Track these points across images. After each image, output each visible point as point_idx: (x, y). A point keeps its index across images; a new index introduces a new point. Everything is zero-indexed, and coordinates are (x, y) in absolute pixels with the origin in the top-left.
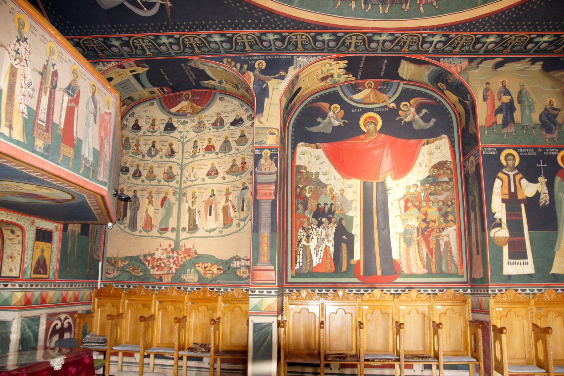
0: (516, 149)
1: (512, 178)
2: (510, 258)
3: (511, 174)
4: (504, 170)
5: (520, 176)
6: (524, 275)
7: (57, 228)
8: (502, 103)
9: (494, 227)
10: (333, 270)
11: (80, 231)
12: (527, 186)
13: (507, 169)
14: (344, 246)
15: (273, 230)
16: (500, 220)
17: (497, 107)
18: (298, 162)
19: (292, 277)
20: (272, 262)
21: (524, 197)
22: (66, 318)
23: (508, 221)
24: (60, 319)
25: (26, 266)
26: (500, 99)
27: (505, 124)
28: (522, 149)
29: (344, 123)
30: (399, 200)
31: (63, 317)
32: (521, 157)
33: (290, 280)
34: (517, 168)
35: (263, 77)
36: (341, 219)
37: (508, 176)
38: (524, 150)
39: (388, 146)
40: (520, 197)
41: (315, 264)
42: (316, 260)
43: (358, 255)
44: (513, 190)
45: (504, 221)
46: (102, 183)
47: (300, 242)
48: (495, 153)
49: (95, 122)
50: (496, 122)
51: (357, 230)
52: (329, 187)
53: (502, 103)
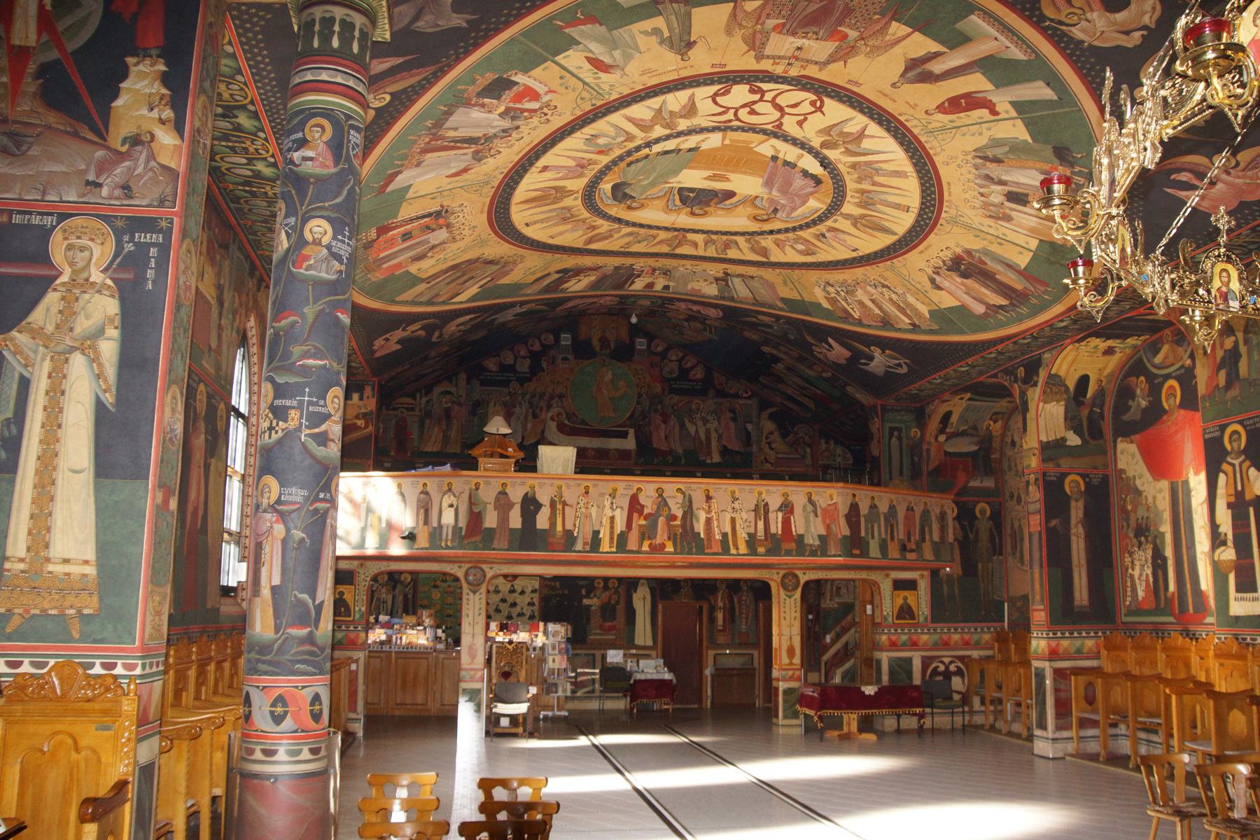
0: (1241, 423)
1: (1237, 468)
2: (1238, 590)
3: (1236, 462)
4: (1229, 459)
5: (1247, 463)
6: (1254, 616)
7: (922, 576)
8: (1225, 351)
9: (1218, 547)
10: (1154, 606)
11: (960, 573)
12: (1256, 479)
13: (1233, 456)
14: (1160, 572)
15: (1041, 566)
16: (1226, 534)
17: (1218, 360)
18: (1121, 465)
19: (1125, 615)
20: (1042, 600)
21: (1252, 497)
22: (951, 662)
23: (1234, 536)
24: (943, 662)
25: (885, 613)
26: (1222, 346)
27: (1228, 386)
28: (1249, 419)
29: (1150, 401)
30: (1201, 504)
31: (947, 660)
32: (1248, 433)
33: (1125, 619)
34: (1245, 452)
35: (1024, 386)
36: (1156, 537)
37: (1233, 465)
38: (1251, 422)
39: (1187, 426)
40: (1248, 497)
41: (1140, 598)
42: (1141, 594)
43: (1172, 587)
44: (1239, 488)
45: (1230, 536)
46: (835, 556)
47: (1127, 570)
48: (1218, 434)
49: (816, 516)
50: (1218, 385)
51: (1169, 552)
52: (1144, 494)
53: (1225, 351)
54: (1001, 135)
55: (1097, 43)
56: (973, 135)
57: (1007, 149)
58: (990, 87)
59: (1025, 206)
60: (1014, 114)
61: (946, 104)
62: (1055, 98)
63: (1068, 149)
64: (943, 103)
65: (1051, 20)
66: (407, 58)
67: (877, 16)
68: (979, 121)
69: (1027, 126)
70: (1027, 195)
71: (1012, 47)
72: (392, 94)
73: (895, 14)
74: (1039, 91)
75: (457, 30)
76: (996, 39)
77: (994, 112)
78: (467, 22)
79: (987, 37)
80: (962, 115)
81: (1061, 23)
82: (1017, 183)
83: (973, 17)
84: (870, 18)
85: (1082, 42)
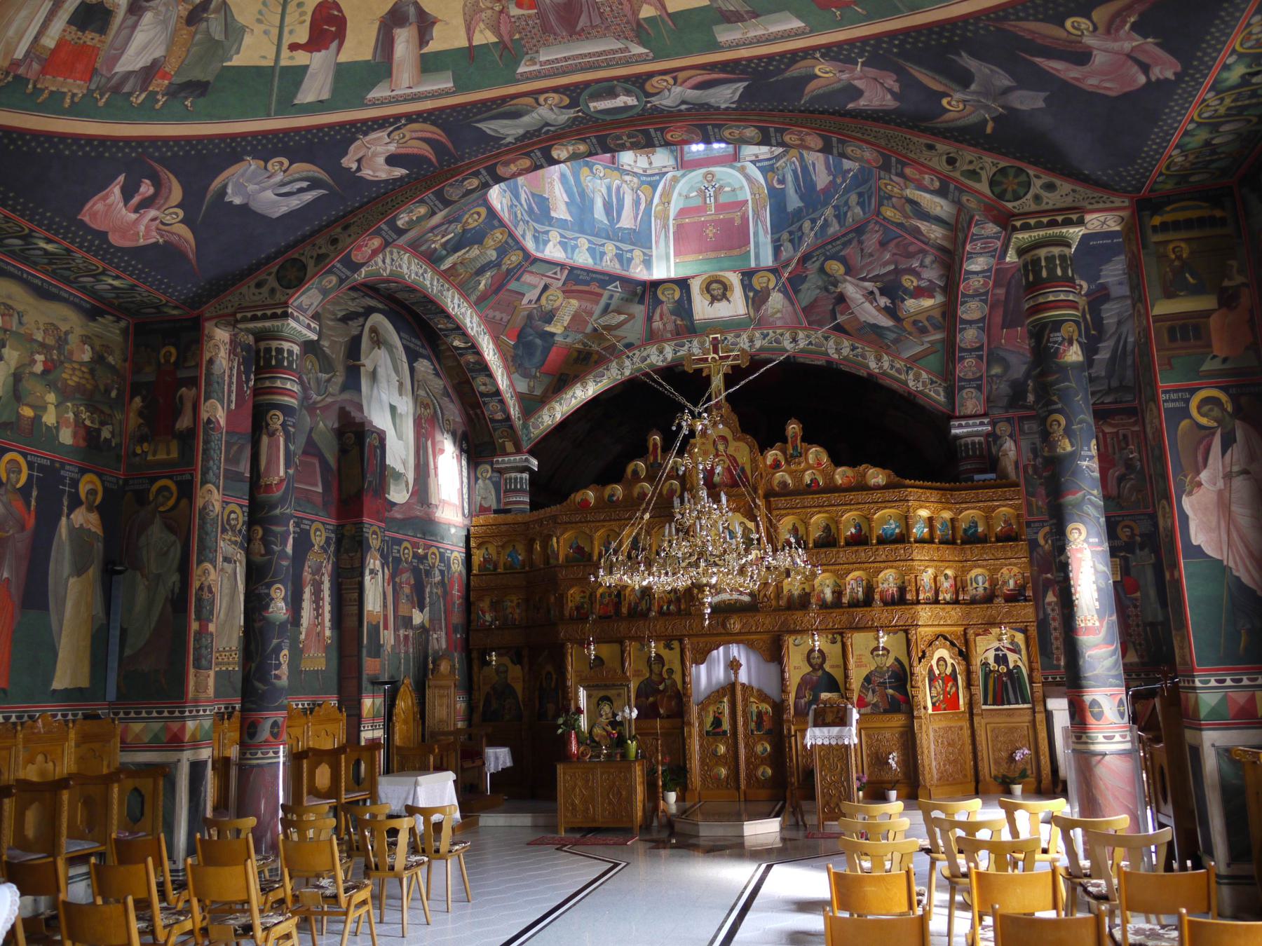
54: (247, 39)
55: (358, 143)
56: (260, 13)
57: (218, 35)
58: (343, 58)
59: (71, 22)
60: (284, 63)
61: (336, 13)
62: (296, 102)
63: (203, 94)
64: (340, 10)
65: (405, 125)
66: (1028, 57)
67: (517, 36)
68: (286, 30)
69: (258, 70)
70: (102, 30)
71: (388, 93)
72: (1062, 25)
73: (505, 47)
74: (310, 92)
75: (974, 55)
76: (410, 88)
77: (294, 47)
78: (960, 56)
79: (419, 83)
80: (308, 18)
81: (398, 128)
82: (134, 27)
83: (450, 85)
84: (520, 33)
85: (366, 134)
